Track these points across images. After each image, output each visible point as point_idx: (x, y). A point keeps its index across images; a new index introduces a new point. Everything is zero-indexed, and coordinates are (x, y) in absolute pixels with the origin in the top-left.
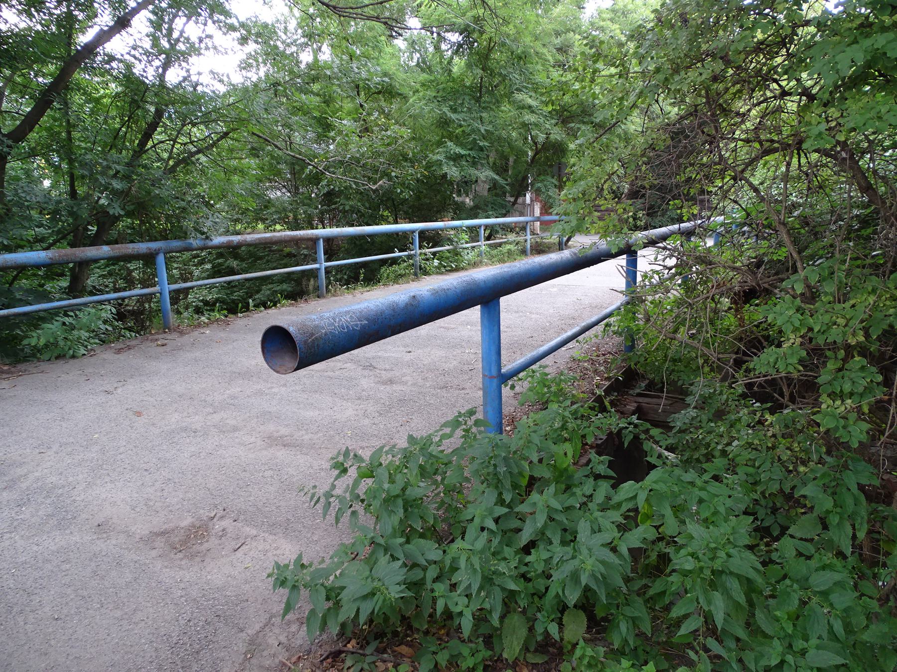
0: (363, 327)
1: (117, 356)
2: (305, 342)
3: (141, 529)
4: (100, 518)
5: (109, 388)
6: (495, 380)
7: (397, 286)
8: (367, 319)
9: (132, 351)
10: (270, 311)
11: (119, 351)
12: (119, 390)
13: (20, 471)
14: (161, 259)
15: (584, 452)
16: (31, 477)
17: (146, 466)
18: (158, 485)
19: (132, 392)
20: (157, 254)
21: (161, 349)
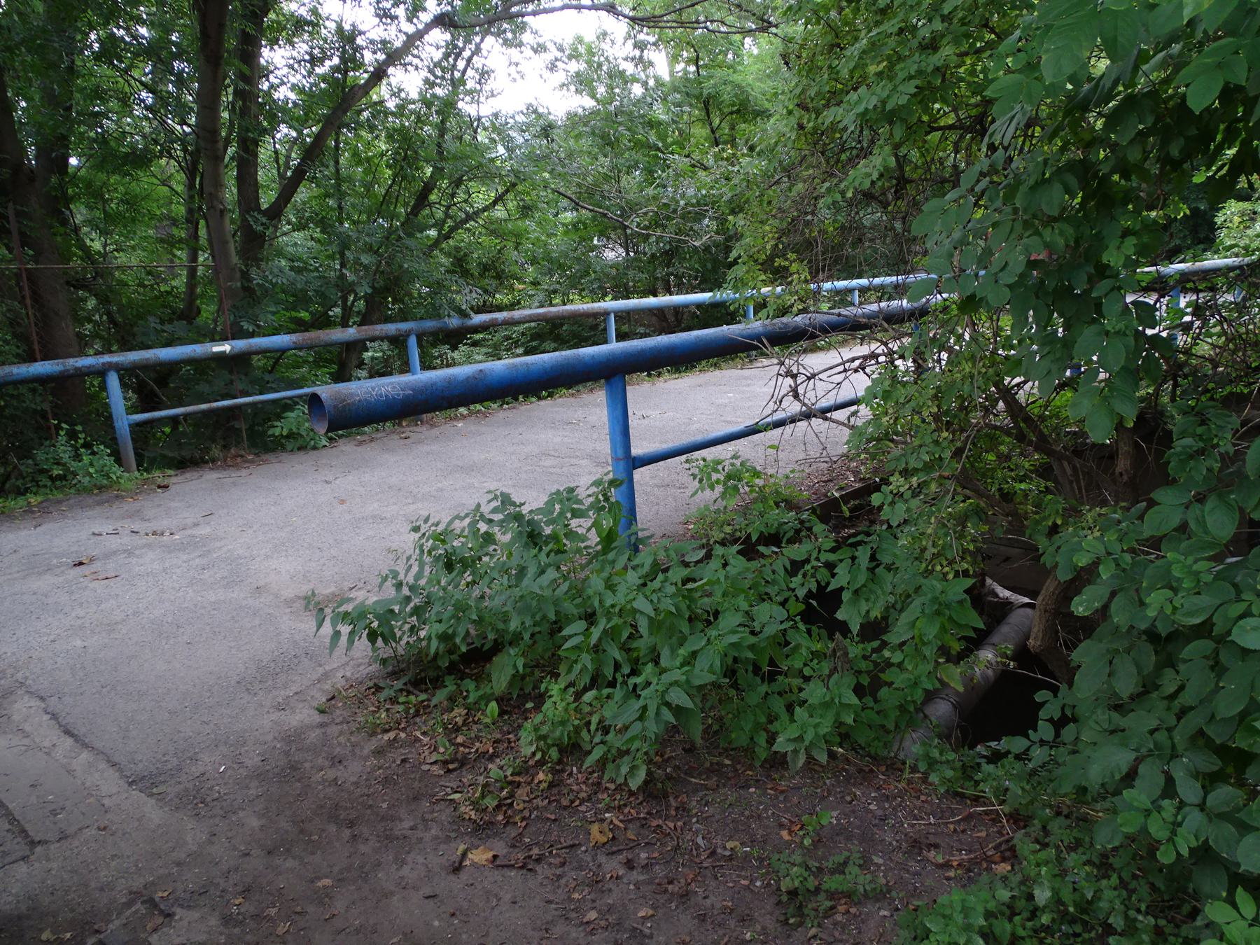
0: (407, 397)
1: (359, 449)
2: (335, 407)
3: (289, 593)
4: (261, 583)
5: (331, 478)
6: (622, 463)
7: (717, 372)
8: (413, 390)
9: (373, 444)
10: (542, 403)
11: (360, 443)
12: (337, 481)
13: (218, 544)
14: (413, 341)
15: (940, 604)
16: (225, 549)
17: (320, 545)
18: (322, 561)
19: (347, 483)
20: (408, 336)
21: (402, 442)
